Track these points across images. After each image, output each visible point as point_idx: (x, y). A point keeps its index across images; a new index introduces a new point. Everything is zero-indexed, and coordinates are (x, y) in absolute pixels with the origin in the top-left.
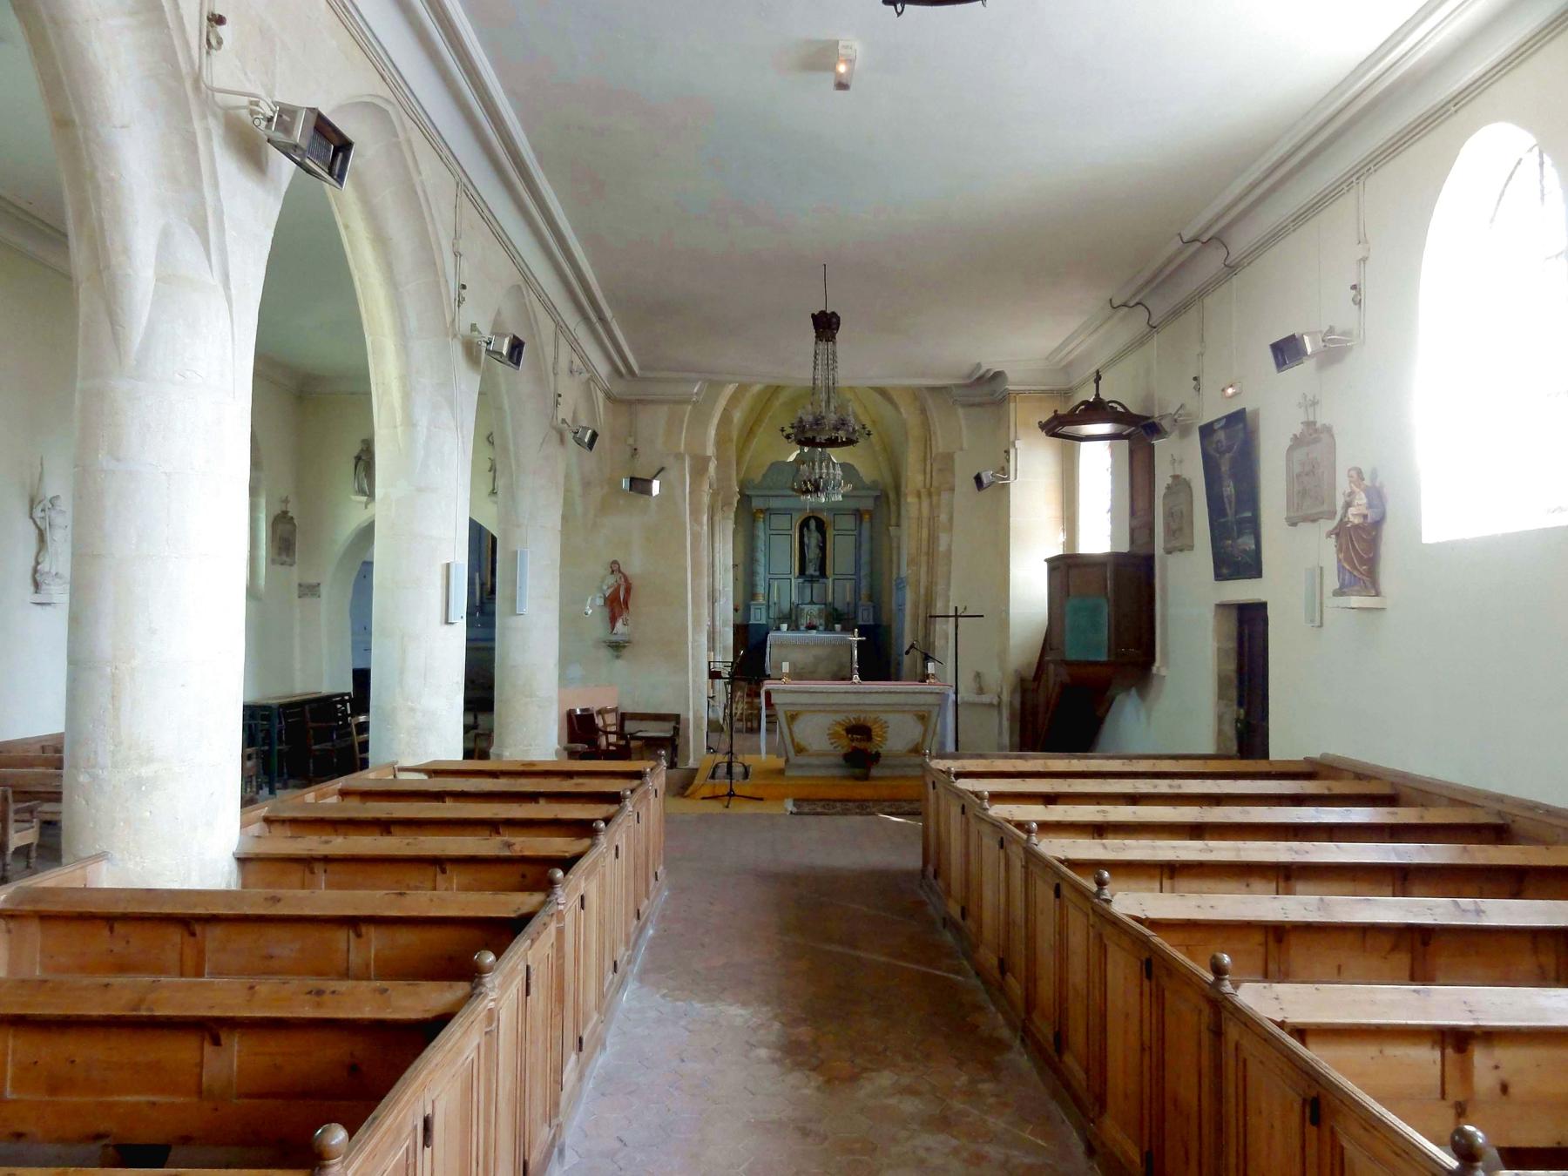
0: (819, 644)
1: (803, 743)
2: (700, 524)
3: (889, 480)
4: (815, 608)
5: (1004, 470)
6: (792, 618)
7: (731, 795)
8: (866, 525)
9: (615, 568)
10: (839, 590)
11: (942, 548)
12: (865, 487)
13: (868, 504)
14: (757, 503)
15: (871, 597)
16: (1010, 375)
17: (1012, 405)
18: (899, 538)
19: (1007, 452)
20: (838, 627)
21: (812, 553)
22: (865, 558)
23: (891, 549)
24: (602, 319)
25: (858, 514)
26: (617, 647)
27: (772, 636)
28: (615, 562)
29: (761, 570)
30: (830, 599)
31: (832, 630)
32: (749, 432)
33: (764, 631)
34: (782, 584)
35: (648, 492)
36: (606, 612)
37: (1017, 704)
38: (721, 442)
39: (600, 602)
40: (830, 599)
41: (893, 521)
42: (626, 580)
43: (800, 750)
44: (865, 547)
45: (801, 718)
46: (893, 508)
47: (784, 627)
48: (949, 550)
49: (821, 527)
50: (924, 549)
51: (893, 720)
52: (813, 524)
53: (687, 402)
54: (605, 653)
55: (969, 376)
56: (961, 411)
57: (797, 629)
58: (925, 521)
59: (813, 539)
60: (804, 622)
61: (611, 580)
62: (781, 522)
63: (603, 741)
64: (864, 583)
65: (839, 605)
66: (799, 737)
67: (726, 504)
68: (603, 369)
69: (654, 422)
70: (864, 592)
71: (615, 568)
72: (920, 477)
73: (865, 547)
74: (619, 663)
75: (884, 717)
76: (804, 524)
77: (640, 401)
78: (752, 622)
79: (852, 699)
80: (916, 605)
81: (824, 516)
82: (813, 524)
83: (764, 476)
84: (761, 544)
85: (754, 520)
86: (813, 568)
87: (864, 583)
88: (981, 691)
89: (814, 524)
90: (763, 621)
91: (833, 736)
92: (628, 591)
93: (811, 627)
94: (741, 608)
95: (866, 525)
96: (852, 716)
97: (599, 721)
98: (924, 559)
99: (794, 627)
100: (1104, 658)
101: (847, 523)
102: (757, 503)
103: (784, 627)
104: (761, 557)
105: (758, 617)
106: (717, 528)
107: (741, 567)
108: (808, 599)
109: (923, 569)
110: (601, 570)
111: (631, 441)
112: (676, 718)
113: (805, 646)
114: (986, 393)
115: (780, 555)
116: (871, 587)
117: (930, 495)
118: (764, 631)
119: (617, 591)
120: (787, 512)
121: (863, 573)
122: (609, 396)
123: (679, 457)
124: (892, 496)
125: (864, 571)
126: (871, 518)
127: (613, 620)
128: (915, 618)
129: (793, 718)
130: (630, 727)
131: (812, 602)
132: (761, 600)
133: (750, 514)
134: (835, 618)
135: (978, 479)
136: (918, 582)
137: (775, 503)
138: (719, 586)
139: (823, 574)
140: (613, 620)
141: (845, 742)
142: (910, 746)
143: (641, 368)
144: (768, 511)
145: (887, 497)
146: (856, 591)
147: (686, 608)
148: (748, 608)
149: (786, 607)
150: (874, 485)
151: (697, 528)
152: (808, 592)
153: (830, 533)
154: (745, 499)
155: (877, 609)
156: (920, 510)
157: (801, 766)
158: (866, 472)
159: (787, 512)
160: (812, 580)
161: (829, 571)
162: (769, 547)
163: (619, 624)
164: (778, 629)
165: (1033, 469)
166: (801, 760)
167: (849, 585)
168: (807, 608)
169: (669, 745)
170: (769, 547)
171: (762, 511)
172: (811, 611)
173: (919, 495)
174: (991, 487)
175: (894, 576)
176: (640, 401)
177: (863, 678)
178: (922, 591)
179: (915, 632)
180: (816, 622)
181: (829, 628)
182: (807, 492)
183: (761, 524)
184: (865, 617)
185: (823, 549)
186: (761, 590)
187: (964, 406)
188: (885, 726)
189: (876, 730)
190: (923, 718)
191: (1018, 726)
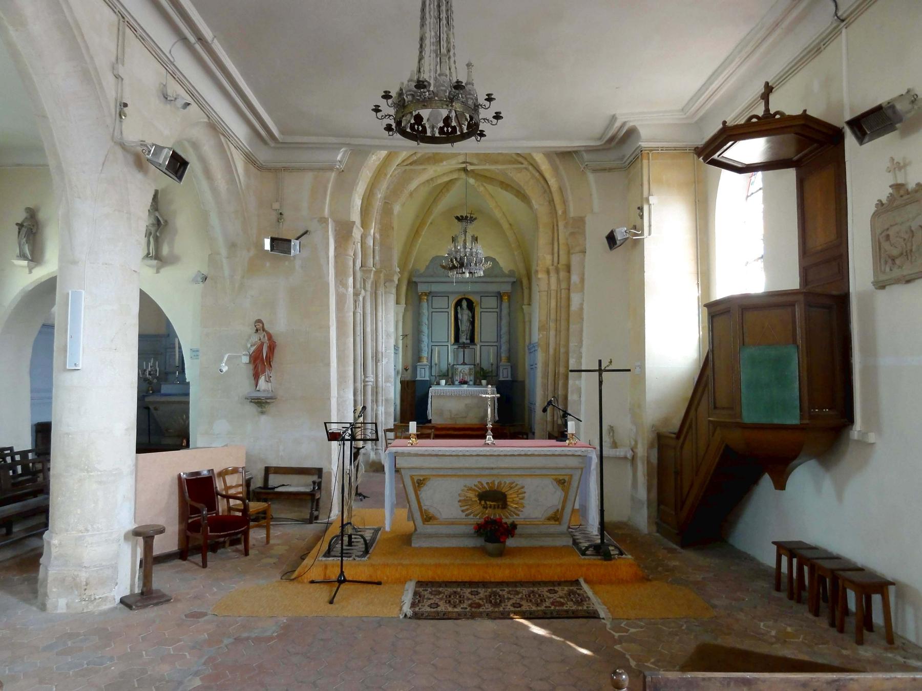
0: (472, 396)
1: (432, 511)
2: (345, 286)
3: (523, 271)
4: (467, 368)
5: (638, 228)
6: (449, 376)
7: (342, 580)
8: (505, 304)
9: (259, 327)
10: (485, 352)
11: (574, 307)
12: (505, 275)
13: (507, 288)
14: (422, 288)
15: (509, 359)
16: (644, 132)
17: (645, 162)
18: (530, 314)
19: (641, 209)
20: (484, 382)
21: (464, 326)
22: (504, 329)
23: (524, 322)
24: (201, 39)
25: (499, 296)
26: (261, 403)
27: (433, 390)
28: (259, 321)
29: (425, 339)
30: (478, 361)
31: (480, 384)
33: (427, 385)
34: (442, 350)
35: (273, 240)
36: (251, 367)
37: (654, 461)
38: (365, 211)
39: (246, 359)
40: (478, 361)
41: (526, 301)
42: (270, 337)
43: (428, 518)
44: (504, 322)
45: (429, 484)
46: (526, 292)
48: (581, 309)
50: (553, 316)
51: (530, 485)
52: (464, 304)
53: (331, 169)
54: (252, 409)
55: (600, 139)
56: (591, 177)
57: (453, 383)
58: (553, 294)
59: (465, 315)
60: (457, 378)
61: (255, 338)
62: (440, 303)
63: (222, 506)
65: (485, 365)
66: (426, 504)
67: (388, 280)
68: (238, 129)
69: (299, 189)
71: (259, 327)
72: (549, 258)
73: (504, 322)
74: (264, 418)
75: (520, 482)
76: (458, 304)
77: (286, 169)
78: (418, 378)
79: (484, 462)
80: (546, 365)
81: (470, 297)
82: (464, 304)
83: (428, 267)
86: (465, 337)
87: (504, 348)
88: (615, 445)
89: (466, 304)
91: (464, 502)
92: (272, 348)
93: (463, 382)
94: (410, 368)
95: (505, 304)
96: (484, 481)
97: (219, 485)
98: (552, 325)
100: (794, 419)
101: (492, 302)
102: (422, 288)
103: (443, 382)
104: (425, 329)
105: (423, 375)
106: (379, 301)
107: (410, 337)
109: (552, 333)
110: (250, 330)
111: (276, 206)
112: (319, 472)
113: (459, 397)
114: (617, 155)
115: (440, 327)
116: (509, 350)
117: (557, 271)
118: (427, 385)
119: (259, 350)
122: (250, 159)
123: (323, 221)
124: (525, 282)
125: (504, 339)
126: (509, 297)
127: (256, 377)
128: (545, 375)
129: (419, 484)
130: (274, 480)
132: (425, 362)
133: (415, 293)
134: (481, 375)
135: (611, 239)
136: (548, 345)
137: (435, 288)
138: (381, 348)
140: (256, 377)
141: (478, 508)
142: (550, 513)
143: (282, 132)
144: (429, 294)
145: (521, 283)
146: (498, 355)
147: (328, 365)
148: (415, 369)
149: (444, 367)
150: (512, 273)
151: (342, 290)
153: (478, 310)
154: (412, 284)
155: (514, 368)
156: (549, 284)
157: (430, 536)
158: (505, 264)
159: (446, 295)
160: (464, 346)
161: (477, 339)
162: (430, 319)
163: (262, 380)
164: (438, 384)
165: (666, 226)
166: (429, 529)
167: (492, 350)
168: (460, 368)
169: (311, 501)
170: (430, 319)
171: (426, 294)
172: (464, 370)
173: (548, 272)
174: (624, 244)
175: (527, 341)
176: (286, 169)
177: (494, 437)
178: (551, 351)
179: (545, 387)
180: (467, 378)
181: (477, 383)
182: (454, 267)
183: (425, 304)
184: (505, 375)
185: (473, 323)
186: (425, 354)
187: (595, 171)
188: (521, 492)
189: (511, 496)
190: (562, 483)
191: (655, 482)
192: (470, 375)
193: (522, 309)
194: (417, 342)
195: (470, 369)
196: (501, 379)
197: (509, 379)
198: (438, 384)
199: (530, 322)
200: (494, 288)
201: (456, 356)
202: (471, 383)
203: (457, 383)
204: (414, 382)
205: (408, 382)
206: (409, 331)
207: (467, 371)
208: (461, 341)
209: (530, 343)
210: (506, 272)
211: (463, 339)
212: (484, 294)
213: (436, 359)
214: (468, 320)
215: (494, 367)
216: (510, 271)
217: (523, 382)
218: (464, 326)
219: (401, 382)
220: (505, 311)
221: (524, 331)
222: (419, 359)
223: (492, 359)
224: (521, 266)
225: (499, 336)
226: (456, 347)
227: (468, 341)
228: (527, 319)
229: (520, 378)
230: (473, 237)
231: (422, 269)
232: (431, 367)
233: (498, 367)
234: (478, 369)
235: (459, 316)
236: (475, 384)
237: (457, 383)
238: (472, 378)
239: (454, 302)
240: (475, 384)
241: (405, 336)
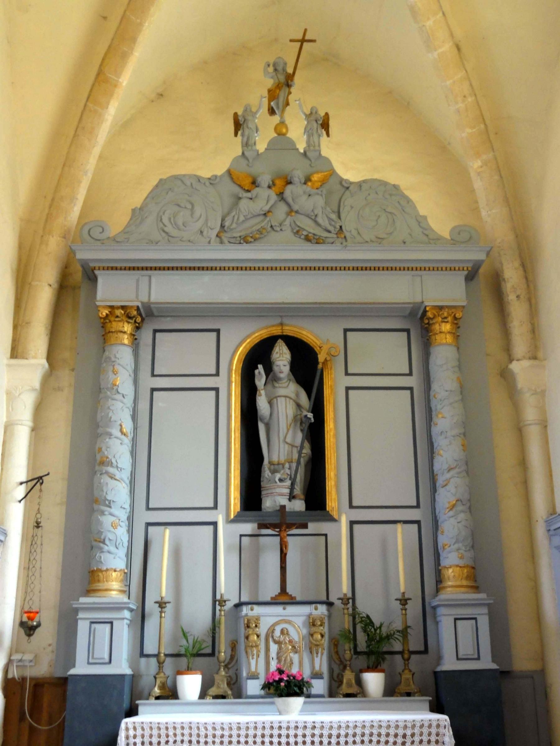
4: (298, 615)
6: (217, 659)
10: (371, 558)
13: (445, 291)
14: (112, 290)
15: (475, 578)
18: (542, 394)
20: (374, 681)
21: (283, 444)
23: (520, 431)
25: (419, 324)
29: (118, 492)
31: (358, 692)
32: (94, 77)
33: (123, 697)
41: (520, 345)
46: (517, 311)
47: (190, 684)
49: (307, 367)
52: (282, 357)
59: (282, 403)
60: (258, 666)
62: (183, 353)
64: (452, 527)
65: (372, 605)
70: (453, 560)
73: (446, 420)
76: (258, 356)
78: (81, 668)
81: (310, 332)
83: (138, 214)
84: (121, 413)
85: (104, 330)
87: (452, 527)
90: (122, 666)
93: (285, 686)
95: (443, 354)
99: (226, 686)
101: (385, 353)
102: (112, 290)
103: (190, 684)
104: (119, 451)
105: (106, 651)
108: (271, 588)
115: (186, 448)
120: (203, 319)
121: (446, 497)
124: (512, 276)
131: (284, 598)
132: (114, 590)
137: (165, 290)
139: (315, 496)
144: (142, 317)
149: (197, 614)
150: (464, 236)
152: (271, 561)
154: (76, 282)
159: (203, 319)
160: (282, 523)
164: (171, 693)
167: (402, 538)
168: (268, 616)
171: (127, 313)
172: (286, 631)
180: (299, 666)
181: (343, 688)
183: (122, 354)
184: (461, 646)
185: (315, 433)
186: (114, 560)
192: (312, 648)
193: (506, 376)
194: (86, 502)
195: (312, 623)
196: (449, 664)
197: (486, 663)
198: (171, 693)
199: (544, 425)
200: (398, 291)
201: (248, 567)
202: (319, 686)
203: (253, 687)
204: (63, 682)
205: (38, 685)
206: (57, 462)
207: (297, 632)
208: (268, 504)
209: (553, 511)
210: (445, 233)
211: (278, 495)
212: (358, 317)
213: (161, 584)
214: (299, 420)
215: (414, 608)
216: (457, 231)
217: (539, 681)
218: (283, 444)
219: (12, 687)
220: (445, 381)
221: (523, 463)
222: (84, 576)
223: (403, 579)
224: (493, 220)
225: (427, 480)
226: (248, 528)
227: (299, 505)
228: (530, 414)
229: (522, 663)
230: (311, 116)
231: (117, 222)
232: (142, 616)
233: (427, 613)
234: (347, 624)
235: (262, 402)
236: (332, 693)
237: (253, 687)
238: (321, 662)
239: (242, 351)
240: (333, 692)
241: (36, 482)
